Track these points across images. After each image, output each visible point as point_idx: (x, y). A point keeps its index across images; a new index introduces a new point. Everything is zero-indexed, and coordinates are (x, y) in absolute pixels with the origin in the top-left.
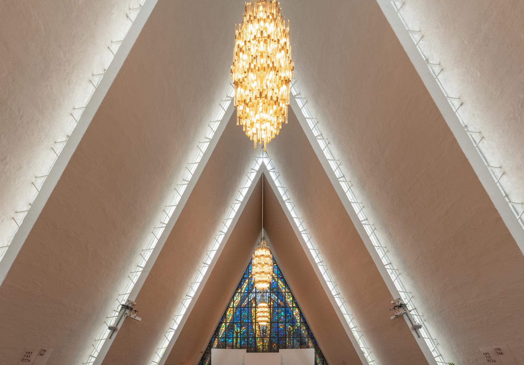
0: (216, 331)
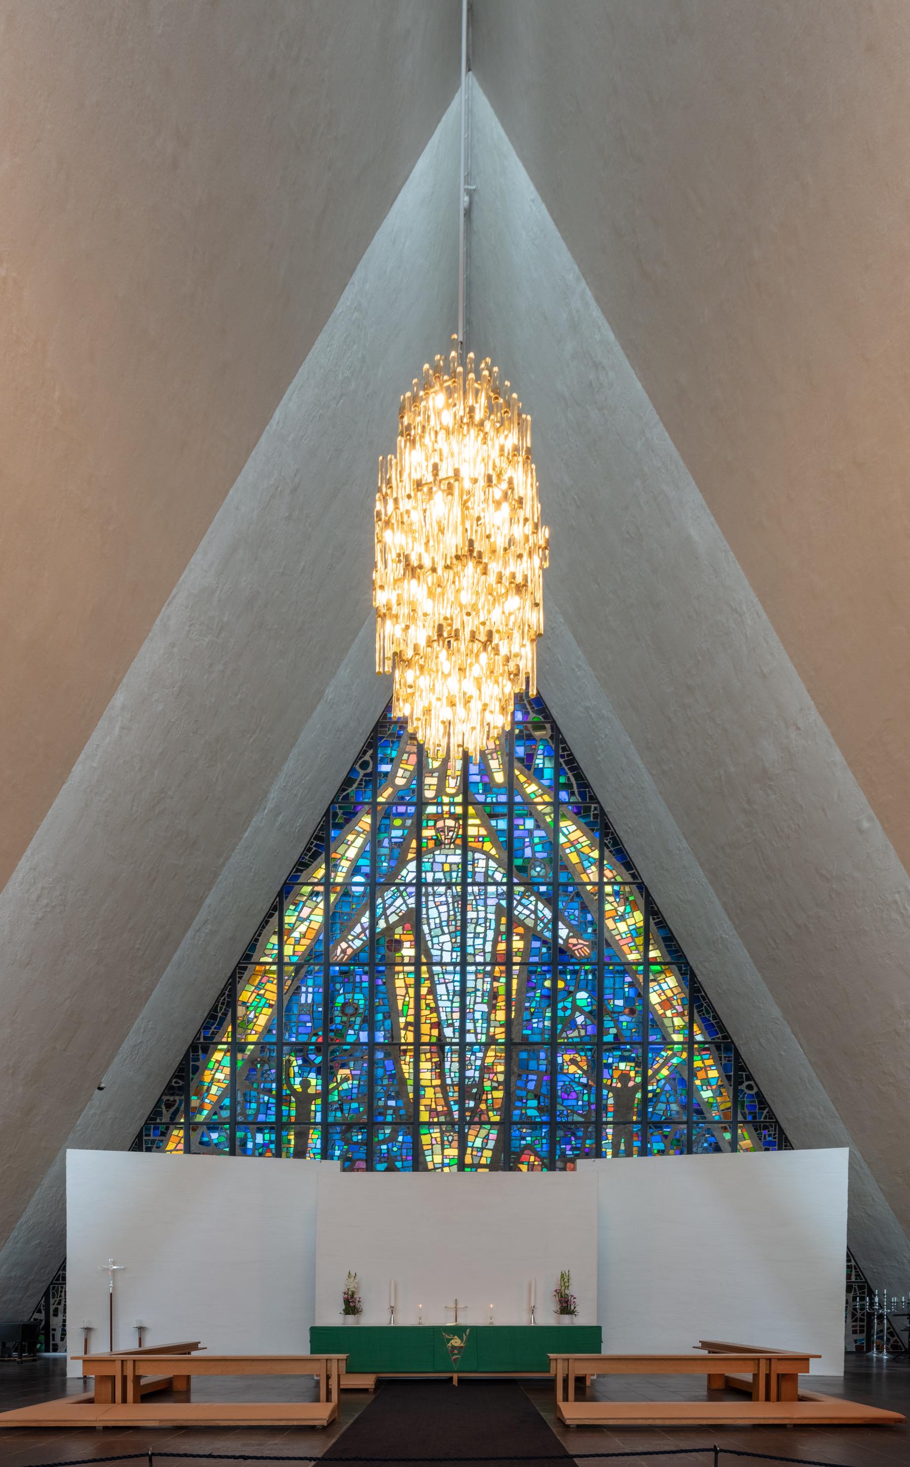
0: (170, 1089)
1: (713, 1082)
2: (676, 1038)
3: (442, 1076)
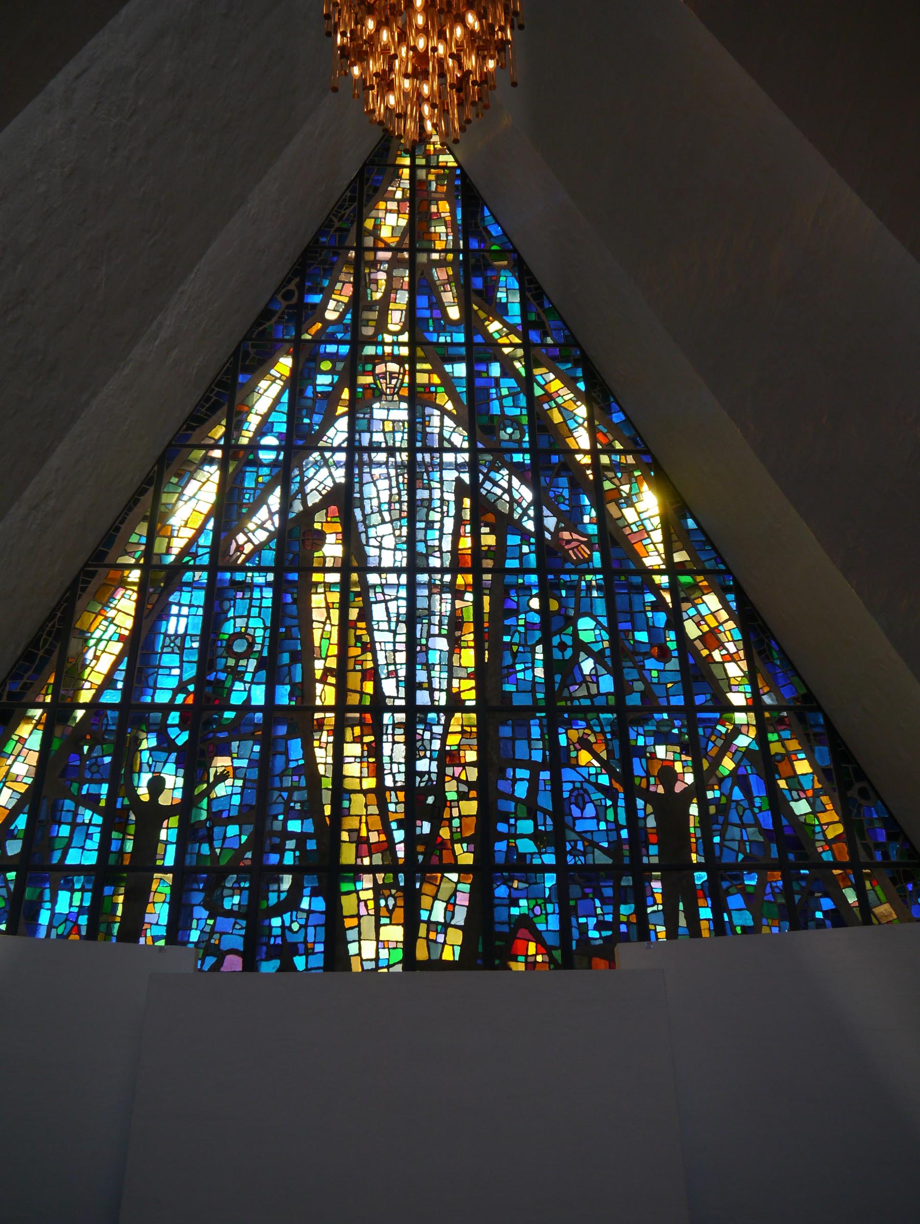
1: (807, 785)
2: (737, 699)
3: (378, 772)
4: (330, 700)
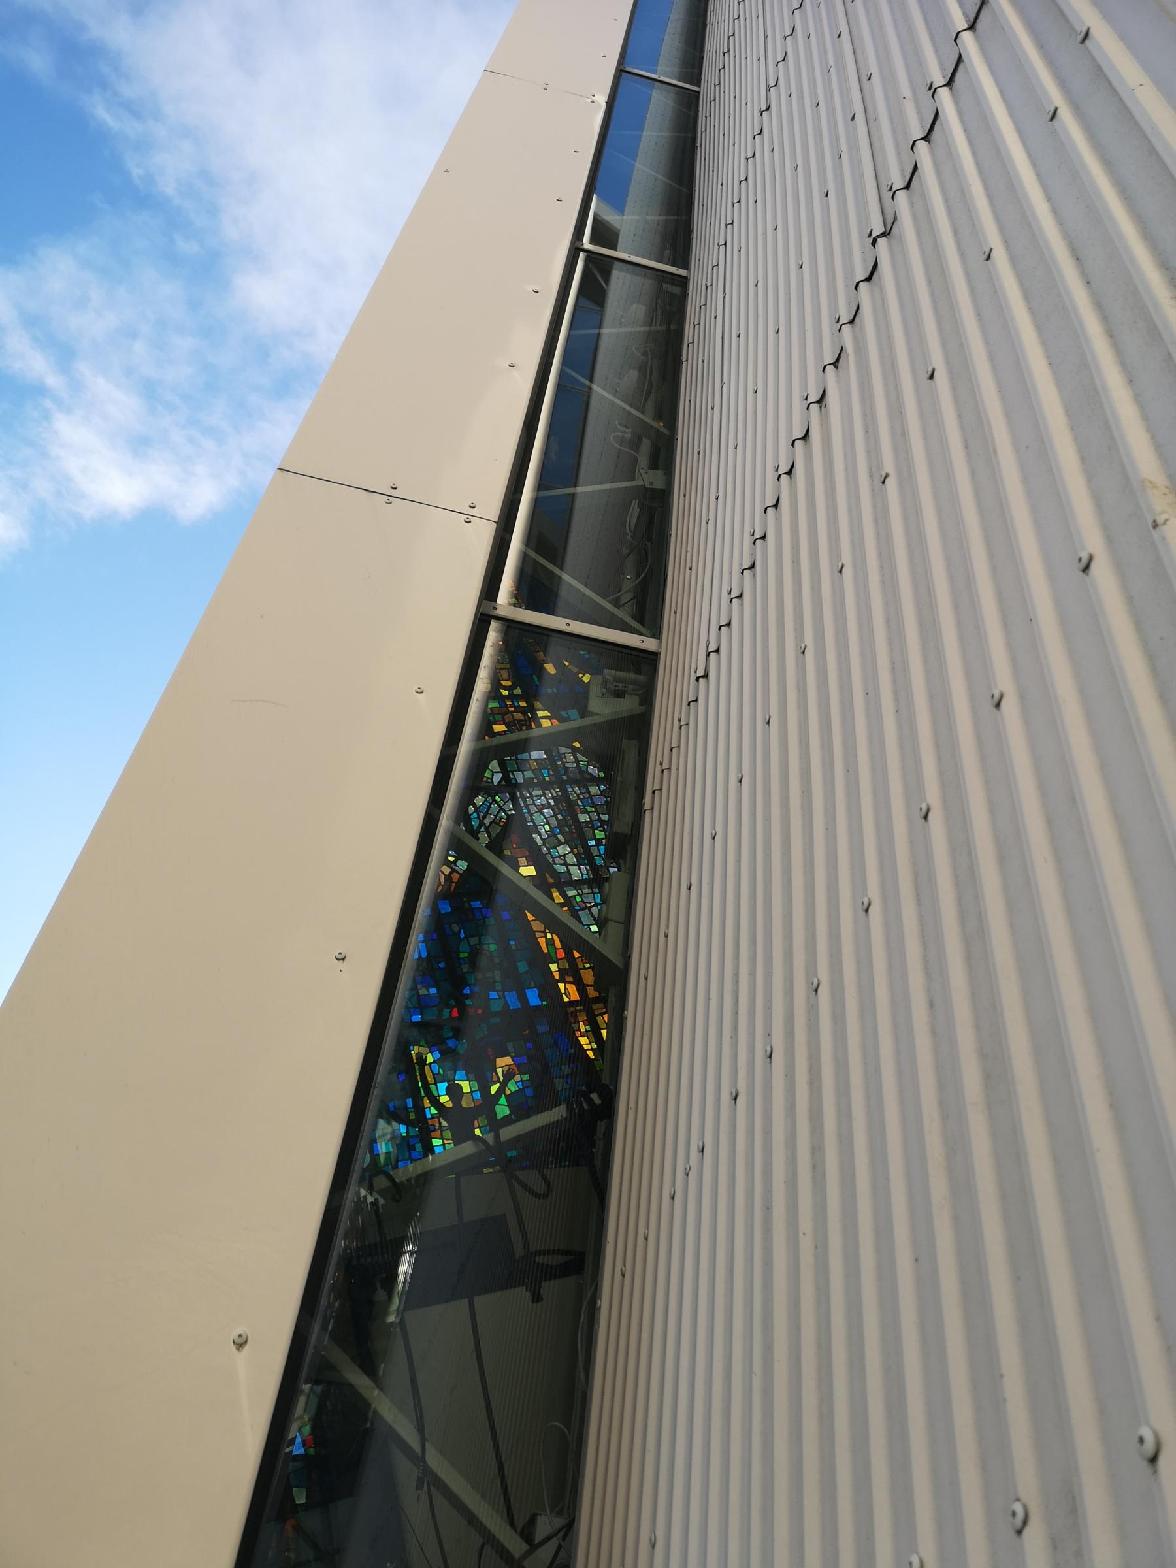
4: (575, 996)
